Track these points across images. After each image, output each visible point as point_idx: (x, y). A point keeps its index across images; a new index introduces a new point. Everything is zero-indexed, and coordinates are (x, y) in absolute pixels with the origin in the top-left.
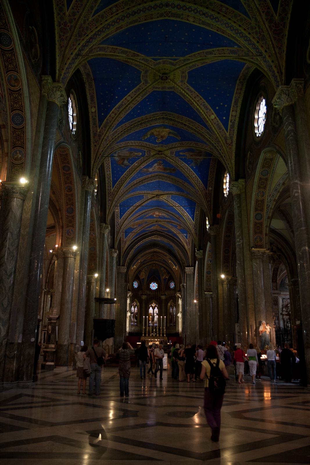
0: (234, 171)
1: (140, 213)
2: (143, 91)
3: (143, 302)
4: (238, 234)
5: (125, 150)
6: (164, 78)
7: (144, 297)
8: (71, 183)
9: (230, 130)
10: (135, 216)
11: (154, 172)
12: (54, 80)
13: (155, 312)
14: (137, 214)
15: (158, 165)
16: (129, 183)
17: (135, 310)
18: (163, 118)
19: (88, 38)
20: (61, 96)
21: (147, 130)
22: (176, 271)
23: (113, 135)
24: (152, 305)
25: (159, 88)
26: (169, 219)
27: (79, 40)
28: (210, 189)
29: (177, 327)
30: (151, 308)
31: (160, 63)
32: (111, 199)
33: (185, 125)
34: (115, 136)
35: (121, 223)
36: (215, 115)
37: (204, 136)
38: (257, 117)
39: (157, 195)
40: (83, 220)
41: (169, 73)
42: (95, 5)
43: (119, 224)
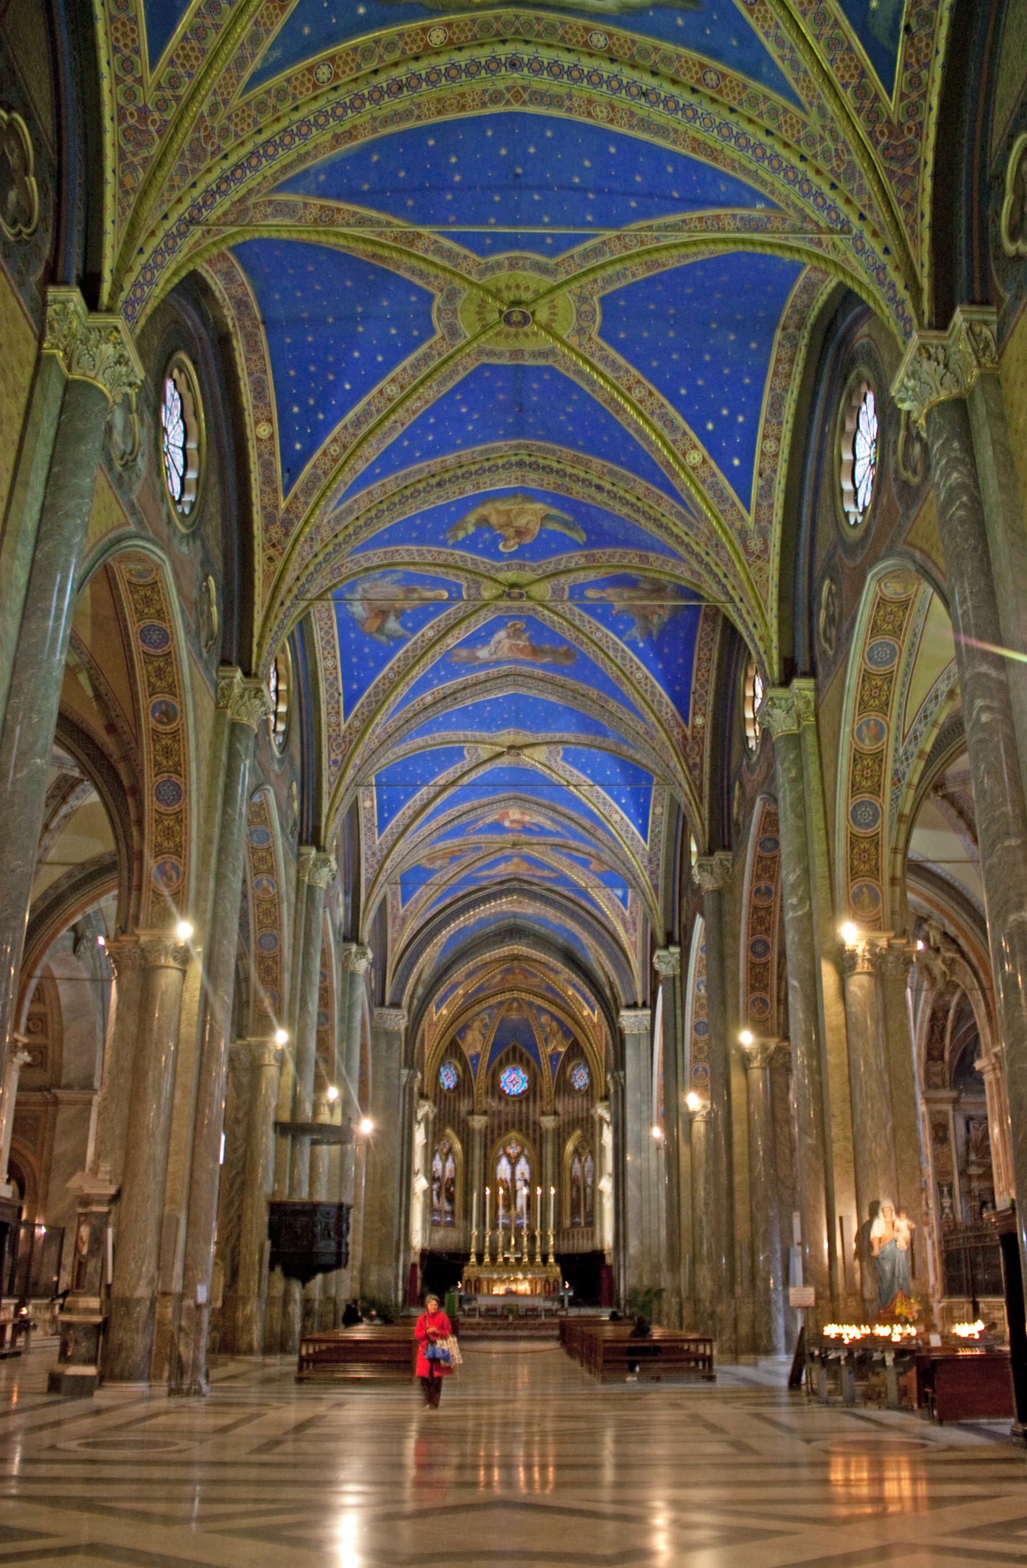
0: (775, 654)
1: (454, 812)
2: (445, 362)
4: (792, 878)
5: (388, 579)
6: (516, 317)
7: (478, 1122)
8: (172, 689)
9: (758, 505)
10: (434, 825)
11: (498, 663)
12: (92, 302)
13: (518, 1175)
14: (442, 819)
15: (509, 637)
16: (406, 700)
18: (521, 464)
19: (226, 164)
20: (118, 362)
21: (466, 505)
22: (594, 1026)
23: (338, 520)
25: (501, 355)
26: (558, 834)
27: (195, 171)
28: (699, 721)
29: (598, 1232)
31: (499, 265)
32: (339, 758)
33: (599, 488)
34: (346, 527)
35: (381, 850)
36: (706, 453)
37: (667, 528)
38: (851, 457)
39: (511, 747)
40: (216, 831)
41: (534, 301)
42: (253, 55)
43: (374, 854)
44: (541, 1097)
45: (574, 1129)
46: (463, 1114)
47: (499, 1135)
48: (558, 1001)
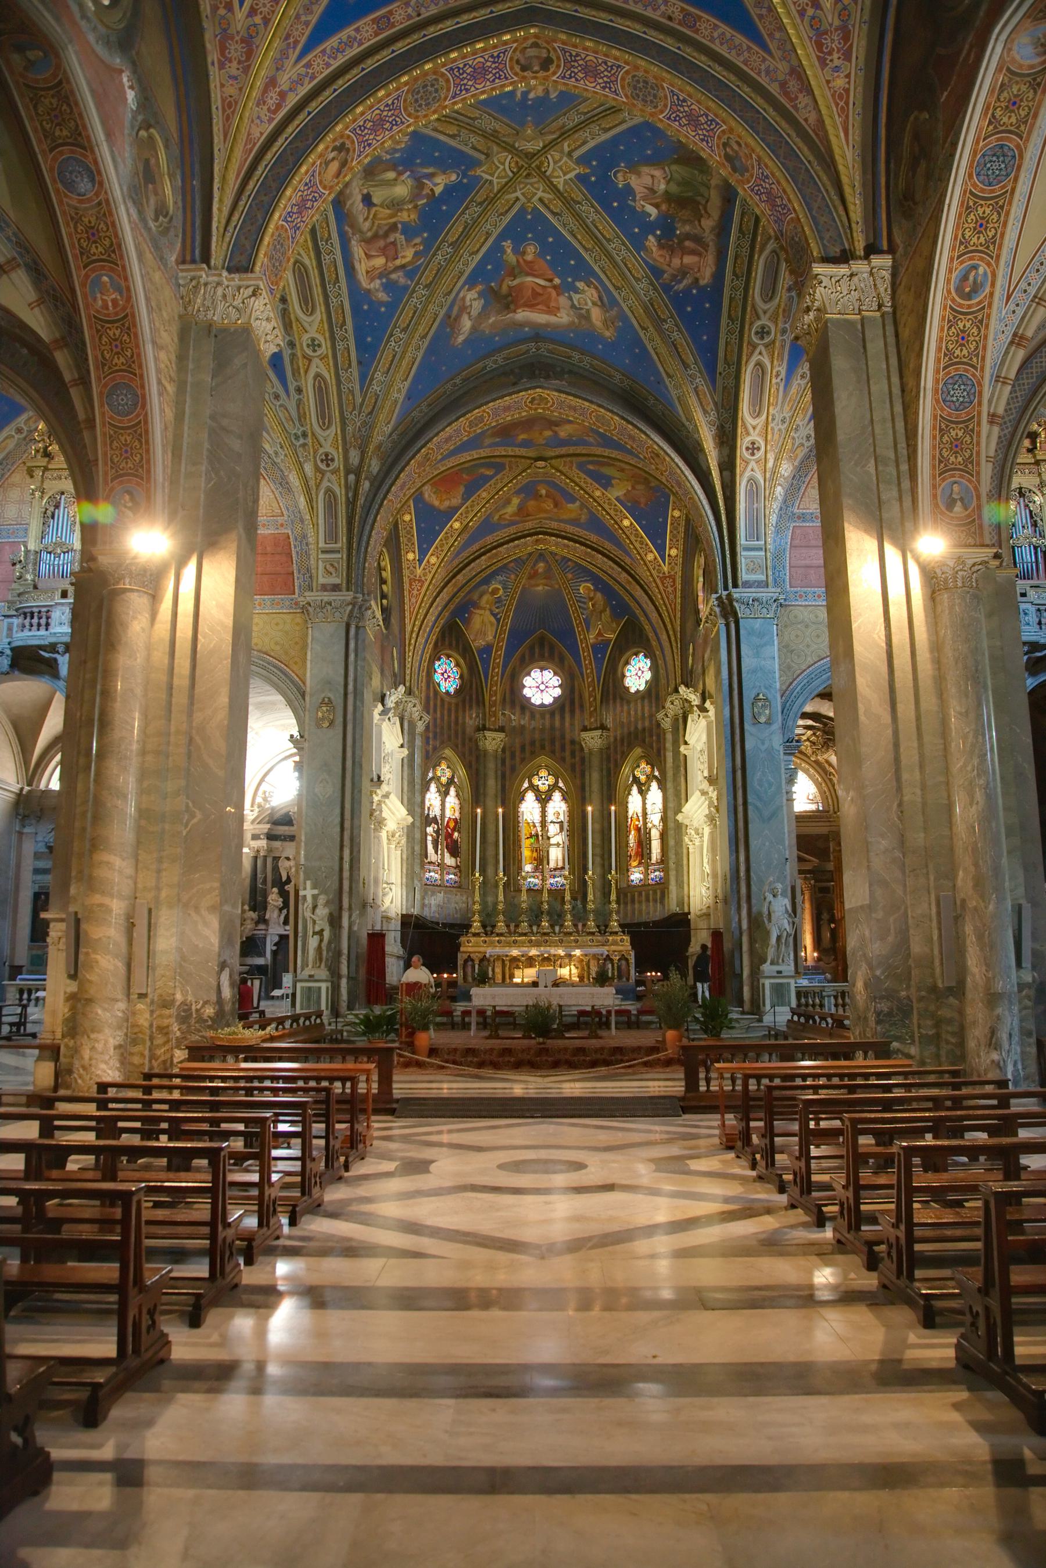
3: (491, 765)
7: (492, 742)
13: (550, 817)
17: (448, 805)
22: (663, 579)
24: (536, 781)
29: (673, 887)
30: (530, 796)
44: (582, 706)
45: (631, 747)
46: (469, 730)
47: (523, 760)
48: (608, 545)
